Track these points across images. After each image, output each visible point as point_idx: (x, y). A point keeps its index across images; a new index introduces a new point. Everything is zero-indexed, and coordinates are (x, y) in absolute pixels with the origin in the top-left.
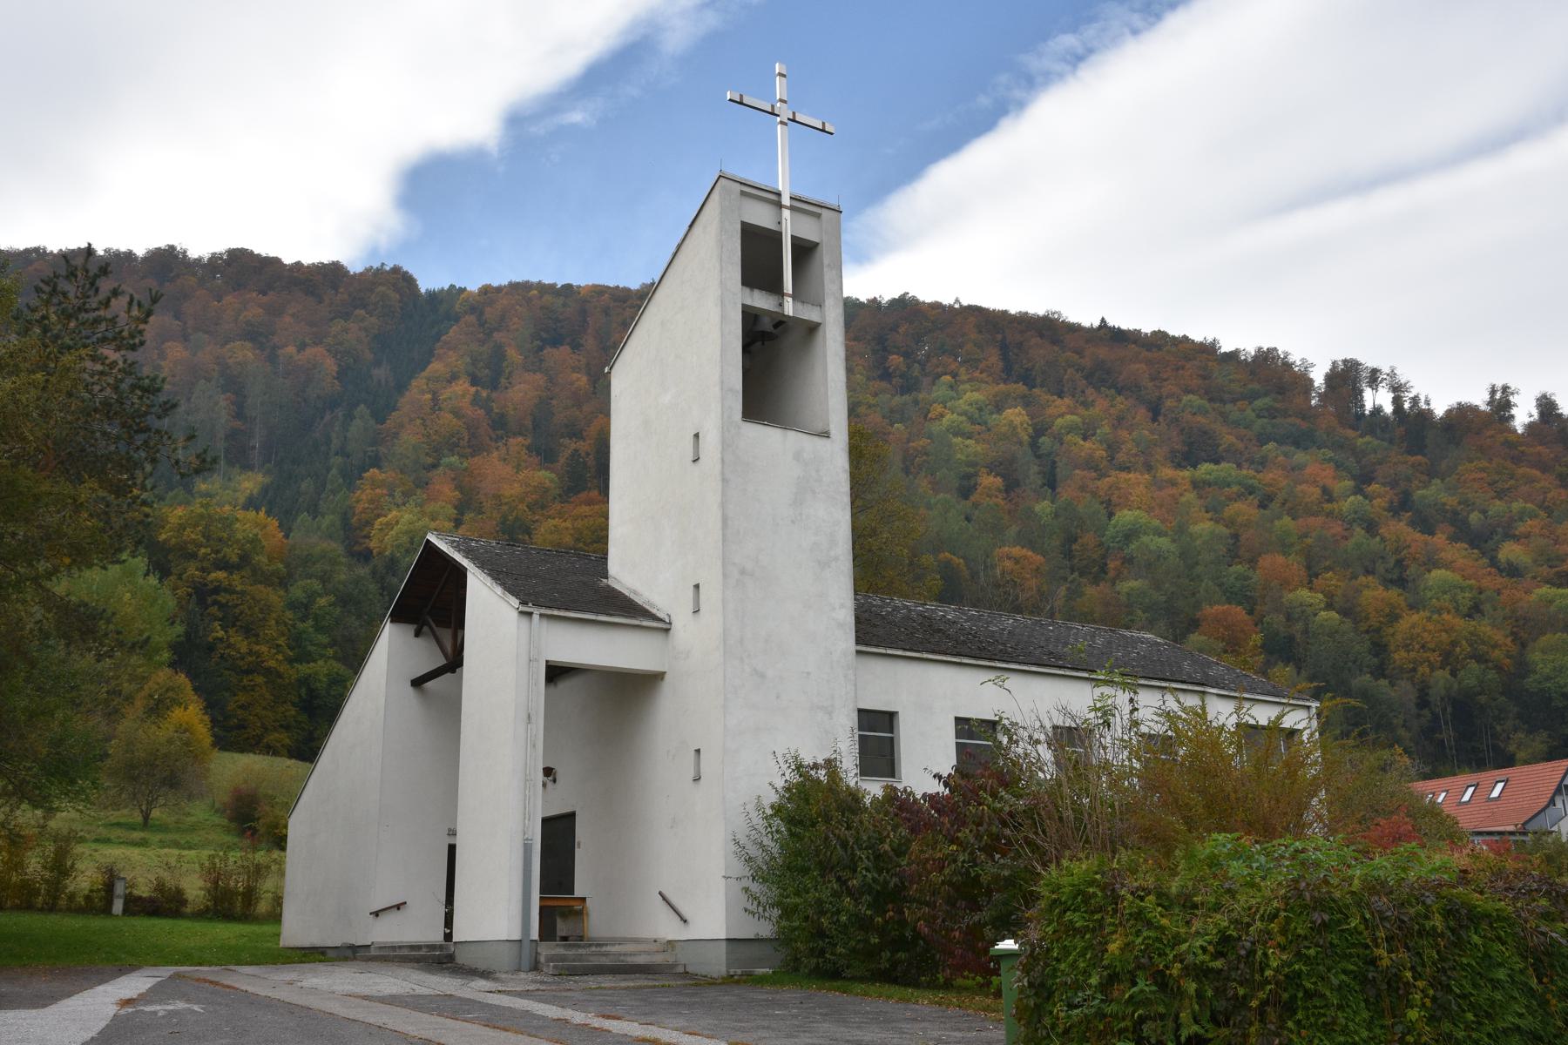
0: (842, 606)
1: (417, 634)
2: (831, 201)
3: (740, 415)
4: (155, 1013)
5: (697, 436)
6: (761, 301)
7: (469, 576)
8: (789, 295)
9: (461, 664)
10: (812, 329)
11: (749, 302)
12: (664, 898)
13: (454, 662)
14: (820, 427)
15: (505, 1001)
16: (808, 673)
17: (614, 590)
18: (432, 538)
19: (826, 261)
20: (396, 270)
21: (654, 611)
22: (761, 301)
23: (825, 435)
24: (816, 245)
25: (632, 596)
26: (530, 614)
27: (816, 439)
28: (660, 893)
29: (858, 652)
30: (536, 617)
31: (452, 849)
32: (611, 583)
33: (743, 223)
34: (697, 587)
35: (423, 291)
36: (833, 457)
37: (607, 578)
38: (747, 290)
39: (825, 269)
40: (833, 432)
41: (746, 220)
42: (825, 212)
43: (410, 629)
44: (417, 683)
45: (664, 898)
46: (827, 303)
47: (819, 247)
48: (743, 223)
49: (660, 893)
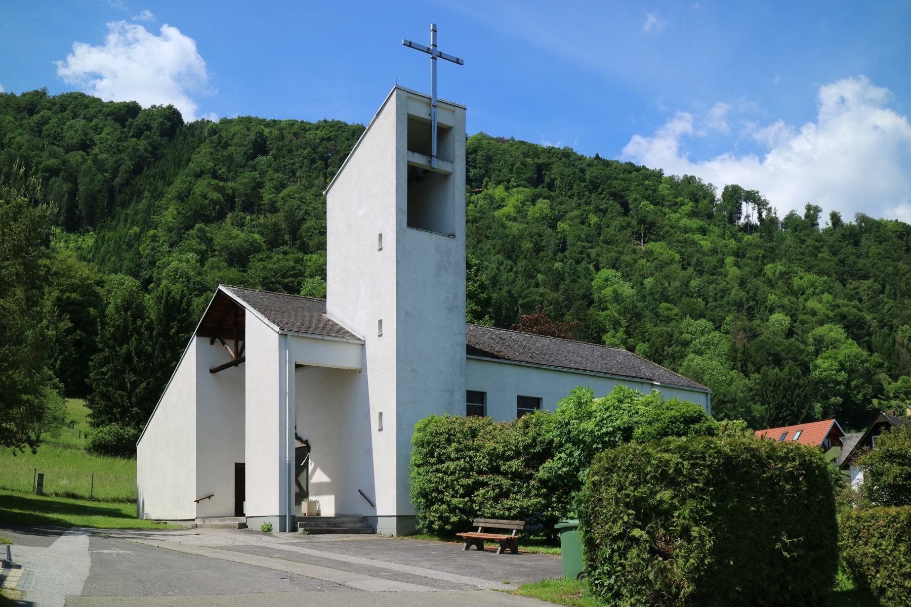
0: (460, 333)
1: (212, 343)
2: (460, 103)
3: (406, 224)
4: (111, 554)
5: (380, 236)
6: (419, 160)
7: (247, 313)
8: (435, 157)
9: (243, 360)
10: (446, 176)
11: (411, 160)
12: (362, 494)
13: (239, 359)
14: (449, 231)
15: (287, 548)
16: (441, 371)
17: (330, 320)
18: (221, 287)
19: (456, 138)
20: (170, 107)
21: (354, 334)
22: (419, 160)
23: (452, 236)
24: (451, 128)
25: (341, 325)
26: (286, 335)
27: (448, 239)
28: (359, 491)
29: (467, 358)
30: (289, 337)
31: (240, 470)
32: (328, 316)
33: (409, 115)
34: (380, 322)
35: (185, 121)
36: (457, 249)
37: (325, 313)
38: (411, 153)
39: (456, 142)
40: (457, 234)
41: (411, 113)
42: (457, 109)
43: (207, 340)
44: (213, 371)
45: (362, 494)
46: (456, 161)
47: (453, 130)
48: (409, 115)
49: (359, 491)
